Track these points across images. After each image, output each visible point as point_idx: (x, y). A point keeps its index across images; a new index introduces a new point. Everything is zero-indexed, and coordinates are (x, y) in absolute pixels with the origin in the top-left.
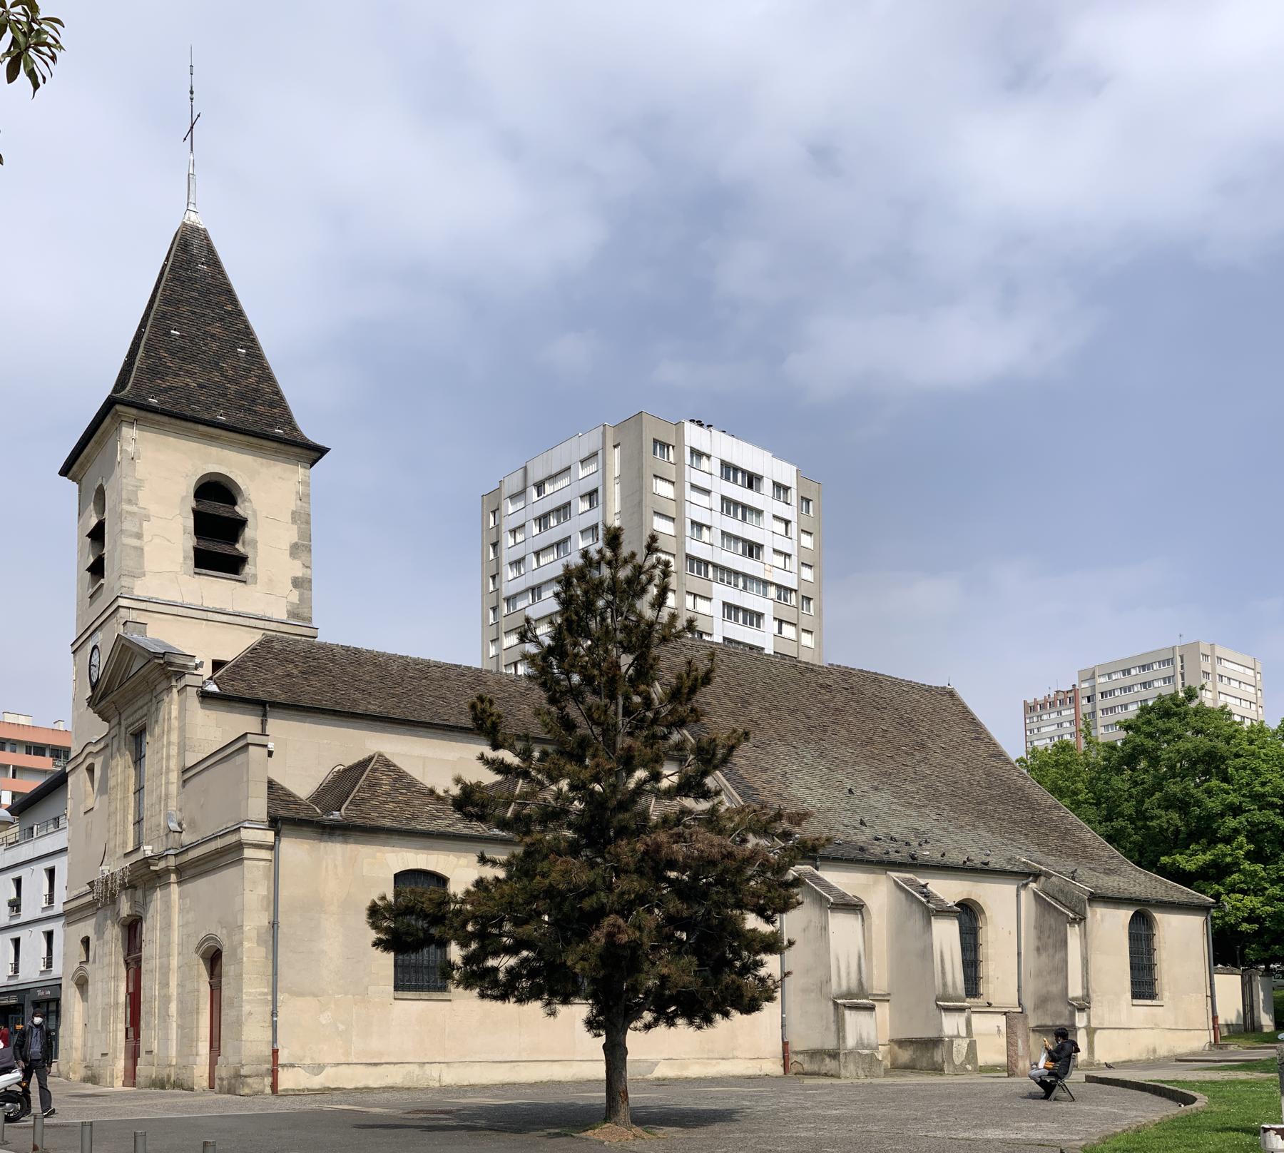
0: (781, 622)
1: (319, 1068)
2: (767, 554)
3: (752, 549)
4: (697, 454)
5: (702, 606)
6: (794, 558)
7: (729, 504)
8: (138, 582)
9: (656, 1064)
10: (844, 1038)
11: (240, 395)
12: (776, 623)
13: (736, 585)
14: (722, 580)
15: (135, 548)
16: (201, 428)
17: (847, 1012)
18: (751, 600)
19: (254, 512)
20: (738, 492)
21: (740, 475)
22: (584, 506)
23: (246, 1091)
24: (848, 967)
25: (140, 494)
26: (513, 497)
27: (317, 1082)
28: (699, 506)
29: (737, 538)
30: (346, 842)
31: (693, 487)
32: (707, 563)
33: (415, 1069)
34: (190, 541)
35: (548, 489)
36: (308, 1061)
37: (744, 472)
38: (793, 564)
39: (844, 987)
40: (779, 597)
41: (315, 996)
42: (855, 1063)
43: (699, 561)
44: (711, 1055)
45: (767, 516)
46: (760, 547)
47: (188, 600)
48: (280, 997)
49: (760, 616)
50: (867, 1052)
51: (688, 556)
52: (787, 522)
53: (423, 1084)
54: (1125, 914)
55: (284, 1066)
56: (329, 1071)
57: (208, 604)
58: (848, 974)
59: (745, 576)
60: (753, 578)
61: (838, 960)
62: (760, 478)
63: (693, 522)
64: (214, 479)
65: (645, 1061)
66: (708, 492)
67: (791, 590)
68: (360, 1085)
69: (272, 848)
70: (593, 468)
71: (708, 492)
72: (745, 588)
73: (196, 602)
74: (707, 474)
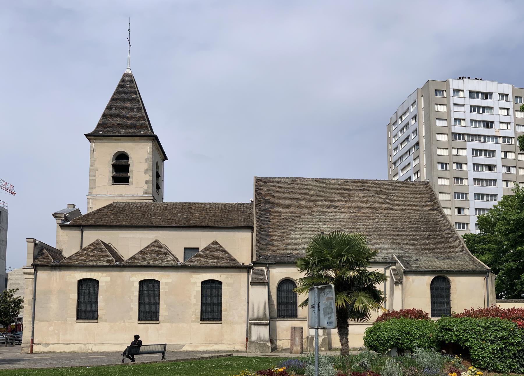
0: (506, 152)
1: (48, 345)
2: (496, 125)
3: (489, 124)
4: (457, 91)
5: (462, 153)
6: (512, 124)
7: (474, 108)
8: (94, 190)
9: (184, 346)
10: (250, 336)
11: (132, 124)
12: (503, 154)
13: (480, 141)
14: (472, 140)
15: (93, 180)
16: (114, 138)
17: (253, 326)
18: (489, 146)
19: (133, 161)
20: (476, 102)
21: (480, 95)
22: (413, 122)
23: (23, 352)
24: (259, 308)
25: (95, 163)
26: (394, 124)
27: (46, 349)
28: (457, 112)
29: (479, 121)
30: (60, 271)
31: (455, 105)
32: (463, 135)
33: (83, 346)
34: (111, 175)
35: (403, 118)
36: (44, 343)
37: (482, 93)
38: (511, 126)
39: (256, 316)
40: (505, 142)
41: (47, 321)
42: (255, 347)
43: (460, 134)
44: (210, 342)
45: (496, 109)
46: (492, 122)
47: (109, 194)
48: (35, 322)
49: (494, 152)
50: (262, 342)
51: (453, 133)
52: (508, 109)
53: (85, 351)
54: (429, 279)
55: (35, 344)
56: (51, 346)
57: (116, 194)
58: (258, 311)
59: (485, 136)
60: (489, 136)
61: (253, 305)
62: (491, 94)
63: (455, 119)
64: (118, 154)
65: (179, 344)
66: (463, 105)
67: (511, 138)
68: (62, 351)
69: (33, 274)
70: (415, 106)
71: (463, 105)
72: (485, 141)
73: (112, 194)
74: (464, 98)
